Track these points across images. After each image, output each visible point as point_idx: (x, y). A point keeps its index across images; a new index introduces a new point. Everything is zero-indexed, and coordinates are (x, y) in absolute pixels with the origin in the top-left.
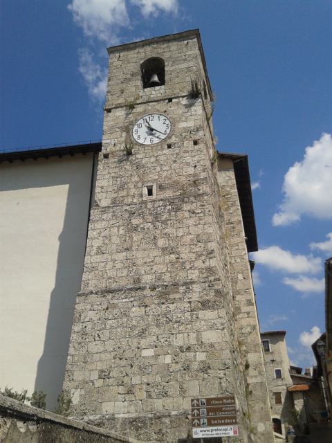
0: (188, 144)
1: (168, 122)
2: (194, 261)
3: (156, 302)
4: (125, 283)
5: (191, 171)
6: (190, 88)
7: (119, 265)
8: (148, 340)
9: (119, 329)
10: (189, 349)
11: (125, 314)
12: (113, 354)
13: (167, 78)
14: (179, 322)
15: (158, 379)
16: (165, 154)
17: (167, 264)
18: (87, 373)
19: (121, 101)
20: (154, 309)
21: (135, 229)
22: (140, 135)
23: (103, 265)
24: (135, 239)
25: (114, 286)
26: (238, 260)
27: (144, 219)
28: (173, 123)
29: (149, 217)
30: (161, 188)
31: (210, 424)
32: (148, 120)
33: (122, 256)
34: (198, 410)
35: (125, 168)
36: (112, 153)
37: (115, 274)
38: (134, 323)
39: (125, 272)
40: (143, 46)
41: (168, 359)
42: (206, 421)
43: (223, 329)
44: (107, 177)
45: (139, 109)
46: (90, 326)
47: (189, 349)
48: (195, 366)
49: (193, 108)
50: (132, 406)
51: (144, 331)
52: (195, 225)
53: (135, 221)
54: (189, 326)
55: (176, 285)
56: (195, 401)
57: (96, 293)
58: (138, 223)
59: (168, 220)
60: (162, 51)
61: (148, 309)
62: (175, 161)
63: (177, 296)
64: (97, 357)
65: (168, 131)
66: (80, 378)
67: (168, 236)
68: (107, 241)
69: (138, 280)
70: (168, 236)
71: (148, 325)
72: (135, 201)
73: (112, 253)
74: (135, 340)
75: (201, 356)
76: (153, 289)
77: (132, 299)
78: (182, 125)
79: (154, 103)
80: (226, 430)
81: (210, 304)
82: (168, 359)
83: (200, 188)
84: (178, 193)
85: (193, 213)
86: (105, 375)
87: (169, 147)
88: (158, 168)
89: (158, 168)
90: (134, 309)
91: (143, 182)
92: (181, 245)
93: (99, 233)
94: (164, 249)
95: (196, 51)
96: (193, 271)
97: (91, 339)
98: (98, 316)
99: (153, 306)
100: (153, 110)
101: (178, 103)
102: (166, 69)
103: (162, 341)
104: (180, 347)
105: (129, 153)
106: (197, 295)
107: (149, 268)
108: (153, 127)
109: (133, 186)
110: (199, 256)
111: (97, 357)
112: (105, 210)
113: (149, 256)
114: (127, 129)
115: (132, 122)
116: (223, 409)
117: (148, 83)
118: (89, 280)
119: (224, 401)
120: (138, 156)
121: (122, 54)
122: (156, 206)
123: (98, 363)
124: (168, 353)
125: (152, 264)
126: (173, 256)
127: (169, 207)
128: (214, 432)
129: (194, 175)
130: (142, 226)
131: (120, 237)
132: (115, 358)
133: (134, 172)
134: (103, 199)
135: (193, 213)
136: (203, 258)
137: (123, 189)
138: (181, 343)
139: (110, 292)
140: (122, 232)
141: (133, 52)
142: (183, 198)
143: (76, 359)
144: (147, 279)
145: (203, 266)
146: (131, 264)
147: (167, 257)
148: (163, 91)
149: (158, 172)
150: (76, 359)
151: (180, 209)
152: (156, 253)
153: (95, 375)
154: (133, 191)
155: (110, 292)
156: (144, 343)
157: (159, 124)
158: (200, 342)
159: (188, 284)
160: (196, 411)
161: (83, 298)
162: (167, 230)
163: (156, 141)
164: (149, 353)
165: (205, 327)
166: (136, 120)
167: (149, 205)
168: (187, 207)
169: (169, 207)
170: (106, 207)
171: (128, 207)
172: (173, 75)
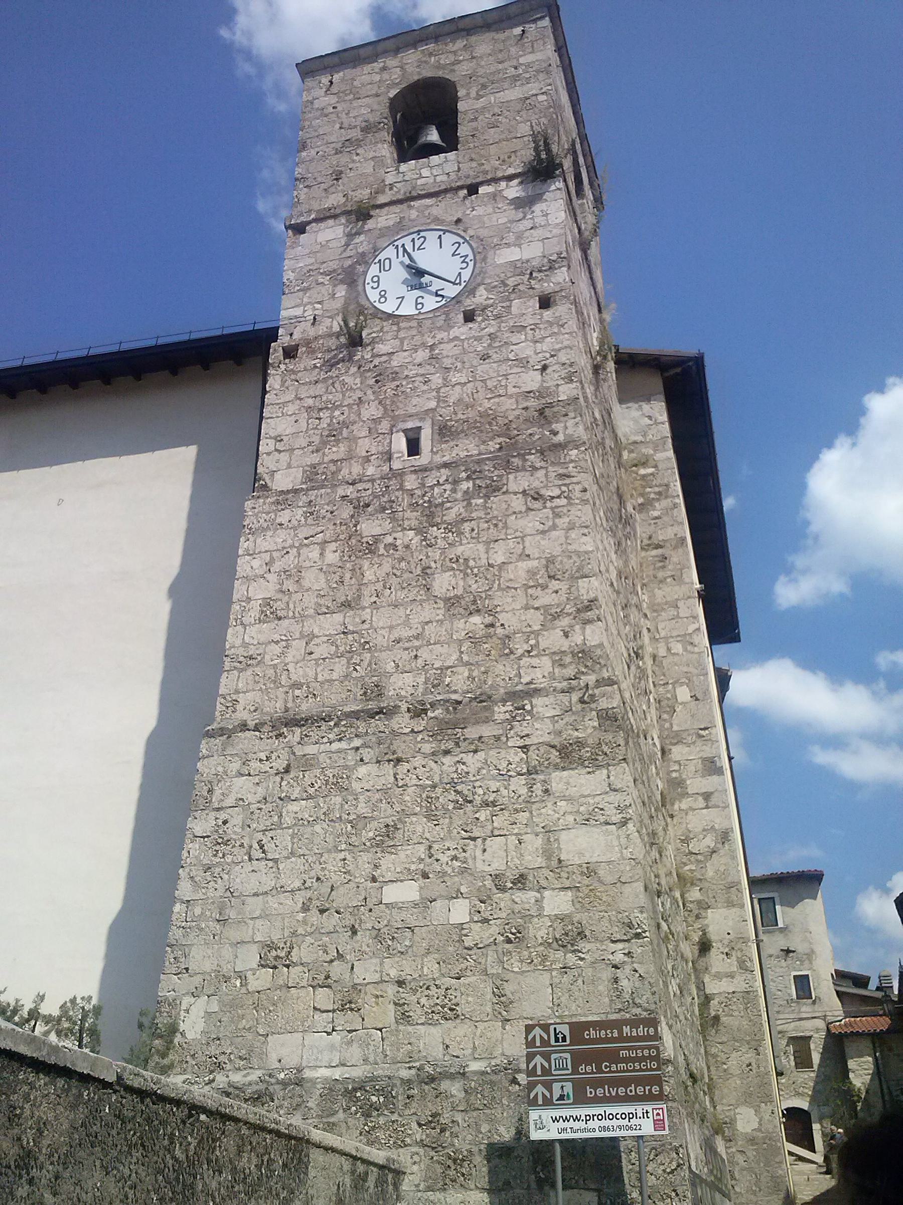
0: (525, 308)
1: (465, 249)
2: (537, 634)
3: (427, 748)
4: (335, 698)
5: (532, 380)
6: (528, 154)
8: (402, 855)
9: (318, 828)
10: (521, 881)
11: (339, 785)
12: (300, 897)
14: (494, 804)
15: (430, 967)
16: (456, 338)
17: (460, 642)
19: (335, 200)
20: (424, 768)
22: (387, 289)
23: (277, 649)
24: (369, 575)
25: (307, 707)
26: (678, 648)
27: (393, 519)
28: (482, 251)
29: (408, 514)
30: (444, 432)
31: (581, 1099)
32: (410, 249)
33: (332, 623)
34: (547, 1056)
35: (344, 384)
36: (308, 343)
37: (311, 673)
38: (363, 809)
39: (340, 668)
40: (397, 51)
41: (460, 912)
42: (569, 1088)
43: (624, 823)
44: (291, 409)
46: (236, 818)
47: (521, 881)
48: (539, 930)
49: (538, 208)
50: (355, 1045)
51: (390, 830)
52: (543, 532)
53: (370, 527)
54: (523, 817)
55: (484, 700)
56: (538, 1031)
57: (256, 729)
58: (377, 531)
59: (464, 520)
60: (452, 58)
62: (485, 357)
63: (487, 731)
64: (254, 905)
65: (466, 275)
66: (208, 966)
67: (462, 565)
68: (289, 585)
69: (379, 690)
70: (462, 565)
71: (404, 813)
72: (371, 471)
74: (365, 857)
75: (557, 903)
76: (418, 712)
77: (357, 742)
79: (428, 201)
80: (631, 1116)
81: (586, 753)
82: (460, 912)
84: (493, 446)
85: (537, 497)
86: (277, 957)
87: (469, 317)
88: (437, 380)
89: (437, 380)
90: (362, 771)
92: (500, 588)
94: (451, 602)
95: (548, 52)
96: (535, 661)
99: (418, 761)
101: (494, 196)
102: (461, 106)
103: (444, 858)
104: (497, 877)
105: (355, 341)
106: (548, 726)
107: (406, 655)
108: (422, 264)
109: (365, 433)
110: (552, 616)
111: (254, 905)
112: (286, 498)
113: (407, 623)
114: (351, 277)
115: (363, 255)
116: (623, 1053)
117: (409, 147)
118: (237, 692)
119: (626, 1030)
120: (382, 348)
121: (337, 77)
122: (430, 482)
123: (259, 922)
124: (459, 895)
125: (416, 643)
126: (476, 619)
127: (466, 485)
128: (594, 1124)
129: (541, 394)
130: (389, 539)
132: (305, 908)
133: (369, 392)
134: (282, 471)
135: (537, 497)
136: (565, 622)
137: (338, 441)
138: (498, 865)
140: (332, 557)
141: (367, 68)
142: (510, 455)
143: (198, 911)
144: (403, 685)
145: (565, 644)
147: (460, 624)
148: (451, 167)
149: (438, 390)
150: (198, 911)
152: (428, 612)
153: (249, 958)
154: (365, 445)
156: (389, 864)
157: (441, 257)
158: (554, 863)
159: (521, 697)
160: (538, 1060)
161: (218, 741)
162: (459, 550)
163: (431, 303)
164: (405, 892)
165: (570, 819)
166: (376, 251)
167: (411, 482)
168: (517, 482)
169: (466, 485)
170: (288, 492)
171: (349, 491)
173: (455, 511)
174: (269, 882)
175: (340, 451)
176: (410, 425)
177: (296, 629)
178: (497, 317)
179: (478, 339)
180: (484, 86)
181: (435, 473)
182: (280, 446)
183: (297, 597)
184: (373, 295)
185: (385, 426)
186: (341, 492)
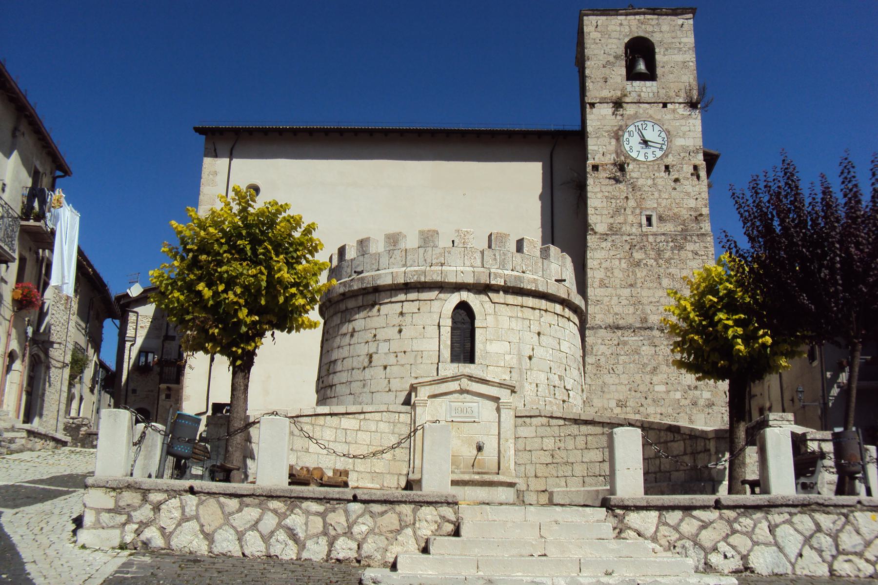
1: (663, 135)
3: (665, 343)
4: (630, 320)
5: (692, 203)
7: (624, 302)
11: (637, 352)
12: (628, 387)
13: (659, 71)
15: (670, 410)
18: (605, 401)
19: (605, 93)
21: (638, 264)
22: (632, 145)
23: (607, 299)
24: (639, 275)
25: (621, 323)
27: (646, 254)
30: (661, 219)
32: (640, 127)
33: (627, 292)
36: (602, 165)
38: (646, 361)
41: (678, 395)
45: (630, 110)
46: (603, 360)
48: (701, 402)
51: (655, 369)
53: (638, 255)
57: (606, 328)
58: (640, 257)
61: (657, 349)
66: (600, 405)
67: (671, 276)
68: (609, 274)
69: (644, 320)
70: (671, 276)
72: (634, 230)
73: (616, 288)
74: (648, 376)
77: (642, 338)
78: (679, 142)
82: (678, 395)
83: (702, 225)
84: (679, 229)
85: (696, 254)
88: (656, 194)
89: (656, 194)
90: (644, 348)
91: (641, 208)
97: (606, 371)
98: (610, 351)
99: (662, 347)
100: (645, 115)
101: (674, 111)
102: (658, 57)
104: (689, 386)
105: (622, 168)
107: (654, 308)
108: (647, 139)
111: (613, 388)
114: (617, 137)
115: (621, 126)
122: (658, 240)
129: (696, 210)
130: (644, 262)
132: (630, 390)
135: (696, 254)
139: (618, 328)
146: (637, 303)
151: (682, 248)
152: (660, 293)
153: (613, 404)
154: (631, 218)
155: (618, 328)
162: (670, 270)
163: (651, 158)
164: (661, 388)
166: (627, 126)
168: (690, 246)
169: (671, 244)
171: (628, 238)
172: (666, 69)
173: (668, 254)
174: (617, 381)
175: (620, 219)
176: (648, 213)
177: (614, 292)
178: (678, 171)
180: (667, 50)
181: (659, 237)
182: (597, 212)
183: (612, 279)
184: (627, 148)
185: (638, 211)
186: (625, 238)
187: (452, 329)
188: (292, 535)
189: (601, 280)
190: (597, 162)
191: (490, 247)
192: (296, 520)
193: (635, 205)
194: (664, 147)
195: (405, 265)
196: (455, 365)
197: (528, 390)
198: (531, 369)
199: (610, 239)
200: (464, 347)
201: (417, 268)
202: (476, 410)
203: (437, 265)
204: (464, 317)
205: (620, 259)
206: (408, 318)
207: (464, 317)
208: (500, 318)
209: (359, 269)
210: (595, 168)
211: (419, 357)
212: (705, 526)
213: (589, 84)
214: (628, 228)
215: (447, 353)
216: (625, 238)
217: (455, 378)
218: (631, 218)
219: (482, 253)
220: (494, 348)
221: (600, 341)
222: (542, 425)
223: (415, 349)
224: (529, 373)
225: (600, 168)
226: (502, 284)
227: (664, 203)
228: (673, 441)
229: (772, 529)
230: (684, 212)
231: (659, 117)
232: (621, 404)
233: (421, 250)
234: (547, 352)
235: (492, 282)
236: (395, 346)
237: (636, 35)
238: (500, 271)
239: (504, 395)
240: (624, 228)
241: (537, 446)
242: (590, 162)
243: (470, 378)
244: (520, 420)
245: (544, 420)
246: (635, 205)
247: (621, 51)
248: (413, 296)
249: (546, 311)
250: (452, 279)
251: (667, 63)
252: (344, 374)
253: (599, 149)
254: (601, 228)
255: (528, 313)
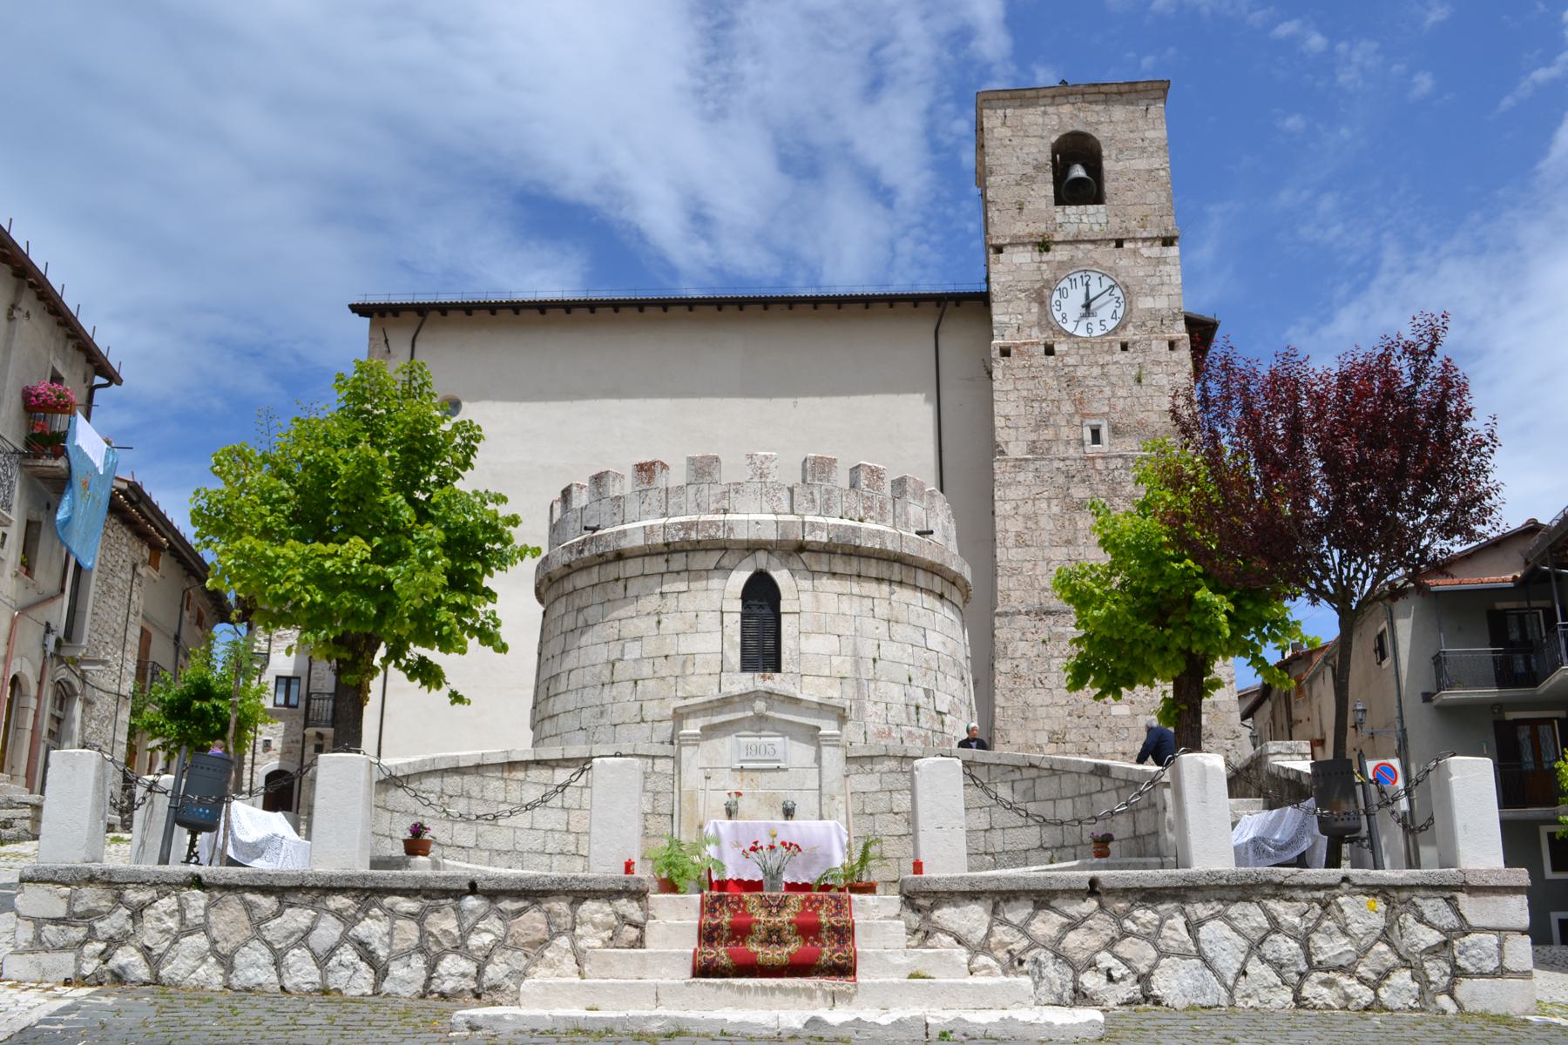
13: (1109, 187)
18: (1030, 734)
19: (1020, 228)
23: (1030, 565)
24: (1080, 525)
30: (1116, 431)
36: (1017, 347)
45: (1060, 254)
46: (1024, 665)
57: (1027, 613)
58: (1082, 495)
64: (1041, 712)
68: (1030, 524)
72: (1071, 452)
73: (1042, 548)
78: (1145, 303)
79: (1090, 246)
87: (1124, 347)
88: (1107, 391)
89: (1107, 391)
93: (1017, 507)
97: (1030, 684)
98: (1036, 651)
111: (1041, 712)
112: (1020, 464)
114: (1040, 297)
115: (1047, 281)
120: (1070, 360)
121: (1008, 111)
122: (1112, 466)
131: (1053, 517)
132: (1070, 715)
139: (1049, 613)
141: (1031, 110)
153: (1042, 738)
154: (1065, 432)
161: (1006, 620)
163: (1097, 332)
166: (1057, 280)
167: (1100, 464)
171: (1061, 464)
172: (1123, 182)
174: (1048, 700)
176: (1094, 422)
177: (1039, 553)
178: (1143, 351)
179: (1132, 365)
180: (1121, 151)
184: (1058, 316)
185: (1077, 420)
186: (1056, 464)
187: (743, 616)
188: (365, 952)
189: (1018, 534)
190: (1007, 342)
191: (804, 481)
192: (372, 928)
193: (1072, 410)
194: (1120, 313)
195: (664, 515)
196: (748, 675)
197: (874, 716)
198: (875, 680)
199: (1032, 467)
200: (762, 648)
201: (683, 519)
202: (779, 749)
203: (717, 512)
204: (761, 599)
205: (1049, 499)
206: (671, 602)
207: (761, 599)
208: (822, 596)
209: (593, 525)
210: (1005, 352)
211: (689, 664)
212: (1073, 925)
213: (993, 214)
214: (1062, 448)
215: (735, 657)
216: (1056, 464)
217: (748, 697)
218: (1065, 432)
219: (791, 490)
220: (815, 645)
221: (1018, 635)
222: (891, 771)
223: (683, 650)
224: (872, 686)
225: (1013, 351)
226: (825, 540)
227: (1120, 404)
228: (1100, 791)
229: (1193, 927)
230: (1154, 418)
231: (1110, 263)
232: (1056, 738)
233: (692, 490)
234: (904, 650)
235: (808, 538)
236: (650, 647)
237: (1070, 129)
238: (820, 519)
239: (828, 728)
240: (1054, 449)
241: (882, 806)
242: (997, 342)
243: (769, 695)
244: (854, 767)
245: (893, 764)
246: (1072, 410)
247: (1045, 156)
248: (678, 562)
249: (901, 583)
250: (741, 535)
251: (1121, 173)
252: (571, 697)
253: (1010, 319)
254: (1016, 450)
255: (870, 588)
